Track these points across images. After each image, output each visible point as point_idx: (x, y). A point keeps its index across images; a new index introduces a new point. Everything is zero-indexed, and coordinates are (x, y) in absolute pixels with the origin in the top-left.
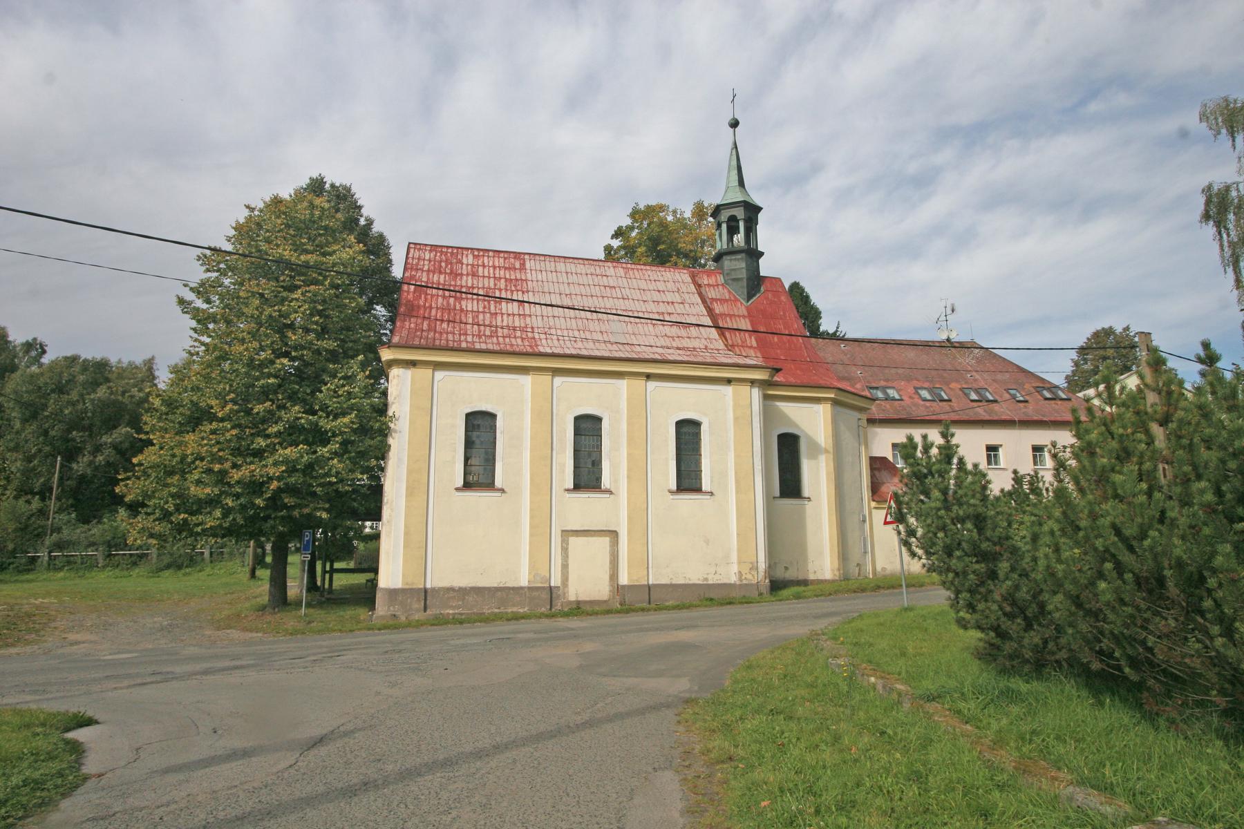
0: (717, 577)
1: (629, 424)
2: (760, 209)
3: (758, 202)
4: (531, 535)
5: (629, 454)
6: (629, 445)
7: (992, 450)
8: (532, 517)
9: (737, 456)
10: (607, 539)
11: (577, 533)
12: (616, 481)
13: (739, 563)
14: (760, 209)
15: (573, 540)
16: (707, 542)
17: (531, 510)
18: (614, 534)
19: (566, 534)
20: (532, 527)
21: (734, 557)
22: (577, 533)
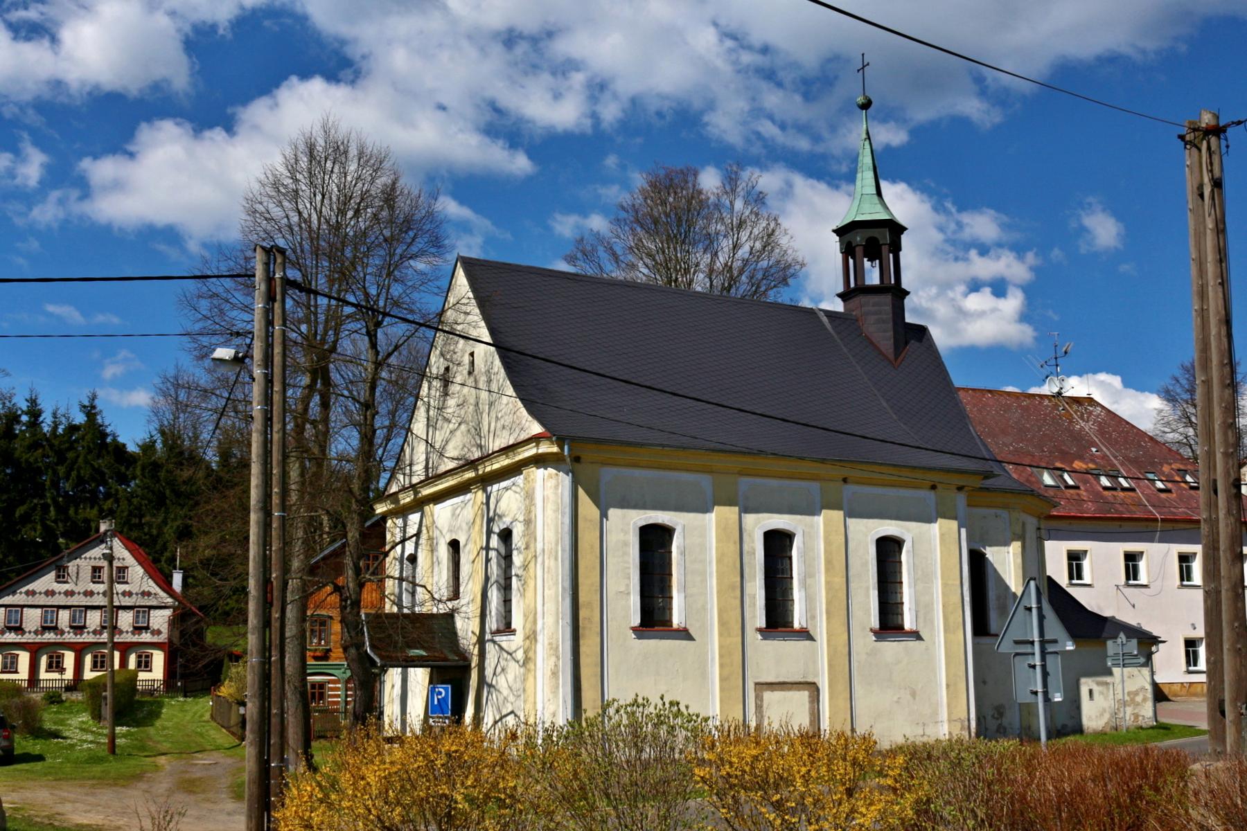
0: (925, 739)
1: (826, 542)
2: (902, 229)
3: (901, 219)
4: (722, 690)
5: (827, 583)
6: (827, 570)
7: (1075, 558)
8: (722, 666)
9: (945, 585)
10: (806, 693)
11: (772, 686)
12: (813, 617)
13: (950, 721)
14: (902, 229)
15: (768, 696)
16: (913, 694)
17: (721, 656)
18: (813, 688)
19: (762, 686)
20: (722, 679)
21: (944, 714)
22: (772, 686)
